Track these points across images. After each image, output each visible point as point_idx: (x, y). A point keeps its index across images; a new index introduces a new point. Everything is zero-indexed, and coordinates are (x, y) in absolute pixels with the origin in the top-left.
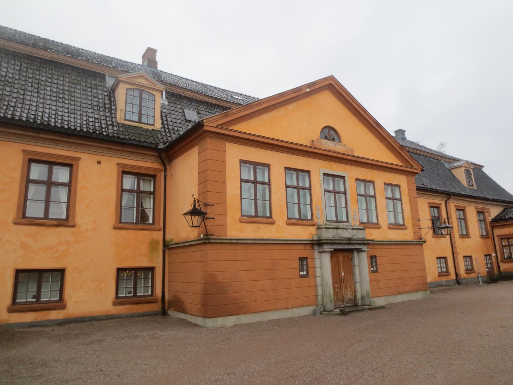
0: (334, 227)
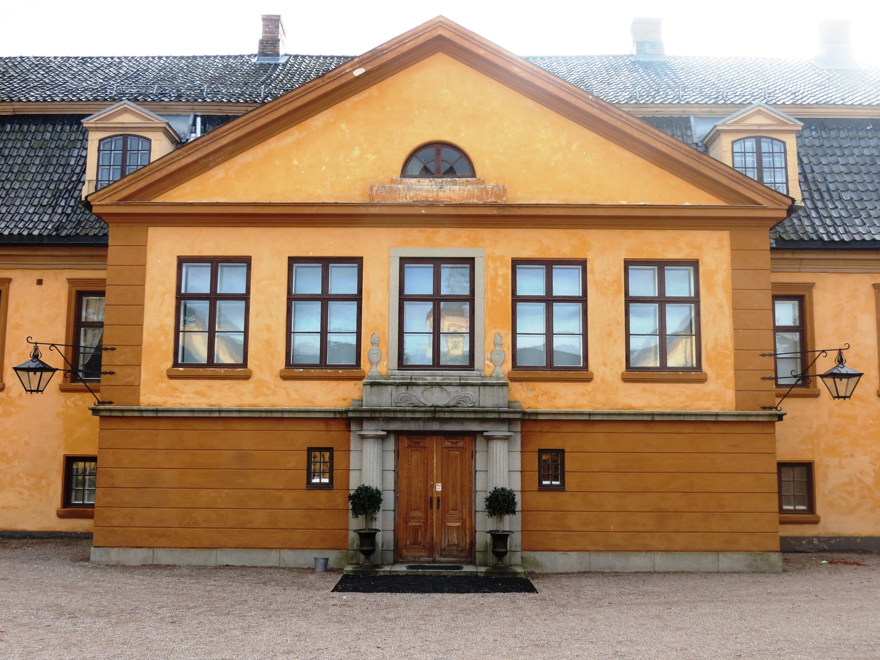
0: (400, 383)
